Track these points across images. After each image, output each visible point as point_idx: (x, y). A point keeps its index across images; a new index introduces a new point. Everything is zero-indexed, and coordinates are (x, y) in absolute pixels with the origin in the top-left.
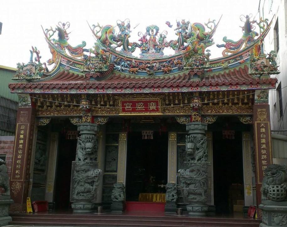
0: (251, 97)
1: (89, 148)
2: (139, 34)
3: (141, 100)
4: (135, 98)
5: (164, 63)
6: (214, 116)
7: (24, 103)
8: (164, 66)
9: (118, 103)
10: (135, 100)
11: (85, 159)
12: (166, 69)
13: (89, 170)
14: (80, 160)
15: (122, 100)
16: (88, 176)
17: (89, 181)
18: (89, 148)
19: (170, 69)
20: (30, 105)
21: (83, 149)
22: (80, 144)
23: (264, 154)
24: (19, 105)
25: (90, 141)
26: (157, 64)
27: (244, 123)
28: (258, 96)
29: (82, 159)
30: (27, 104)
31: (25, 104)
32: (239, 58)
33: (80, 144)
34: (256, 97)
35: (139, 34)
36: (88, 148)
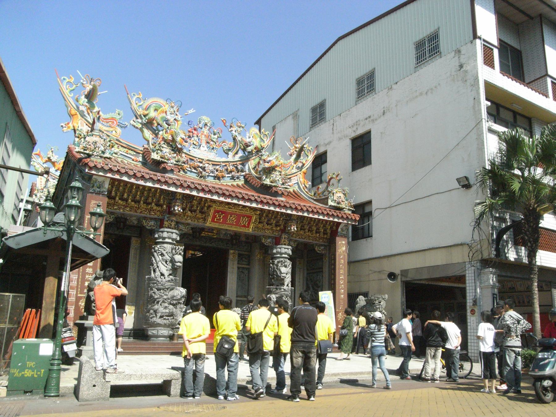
0: (334, 228)
1: (180, 262)
2: (190, 123)
3: (236, 212)
4: (231, 209)
5: (217, 167)
6: (296, 241)
7: (98, 189)
8: (217, 171)
9: (210, 211)
10: (230, 211)
11: (170, 275)
12: (220, 174)
13: (172, 289)
14: (162, 275)
15: (215, 208)
16: (174, 296)
17: (175, 302)
18: (180, 262)
19: (224, 175)
20: (106, 193)
21: (166, 262)
22: (162, 255)
23: (342, 284)
24: (90, 191)
25: (180, 254)
26: (210, 166)
27: (318, 252)
28: (341, 229)
29: (166, 276)
30: (102, 192)
31: (100, 192)
32: (288, 180)
33: (162, 255)
34: (339, 230)
35: (190, 123)
36: (178, 262)
